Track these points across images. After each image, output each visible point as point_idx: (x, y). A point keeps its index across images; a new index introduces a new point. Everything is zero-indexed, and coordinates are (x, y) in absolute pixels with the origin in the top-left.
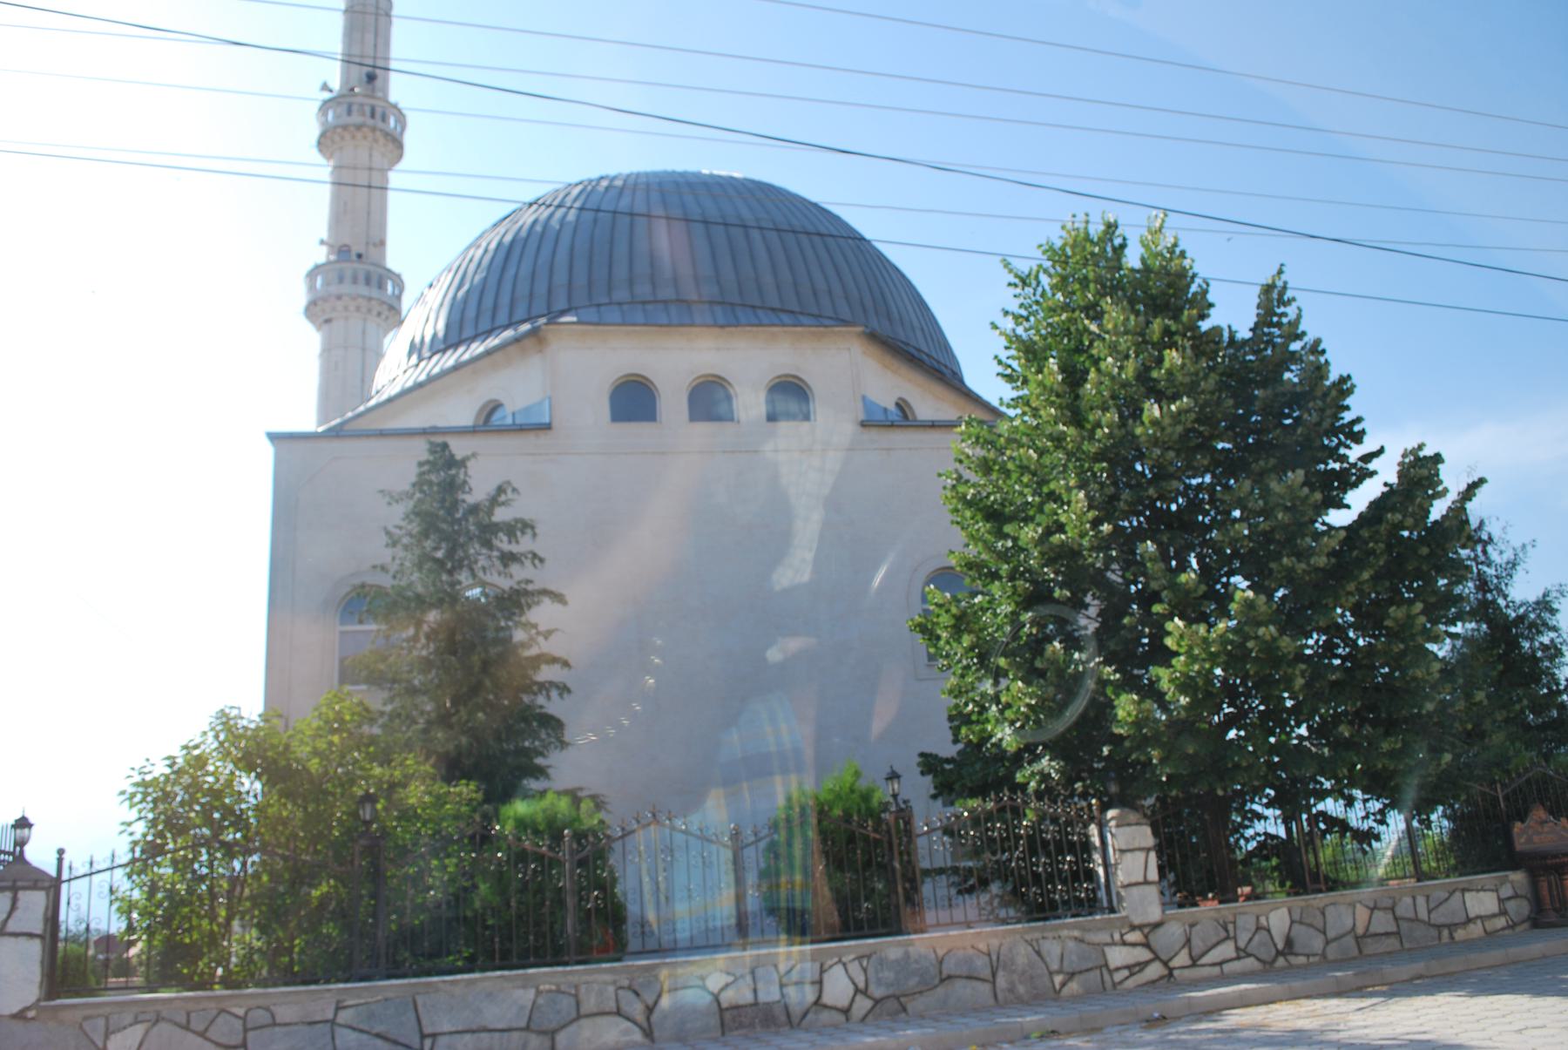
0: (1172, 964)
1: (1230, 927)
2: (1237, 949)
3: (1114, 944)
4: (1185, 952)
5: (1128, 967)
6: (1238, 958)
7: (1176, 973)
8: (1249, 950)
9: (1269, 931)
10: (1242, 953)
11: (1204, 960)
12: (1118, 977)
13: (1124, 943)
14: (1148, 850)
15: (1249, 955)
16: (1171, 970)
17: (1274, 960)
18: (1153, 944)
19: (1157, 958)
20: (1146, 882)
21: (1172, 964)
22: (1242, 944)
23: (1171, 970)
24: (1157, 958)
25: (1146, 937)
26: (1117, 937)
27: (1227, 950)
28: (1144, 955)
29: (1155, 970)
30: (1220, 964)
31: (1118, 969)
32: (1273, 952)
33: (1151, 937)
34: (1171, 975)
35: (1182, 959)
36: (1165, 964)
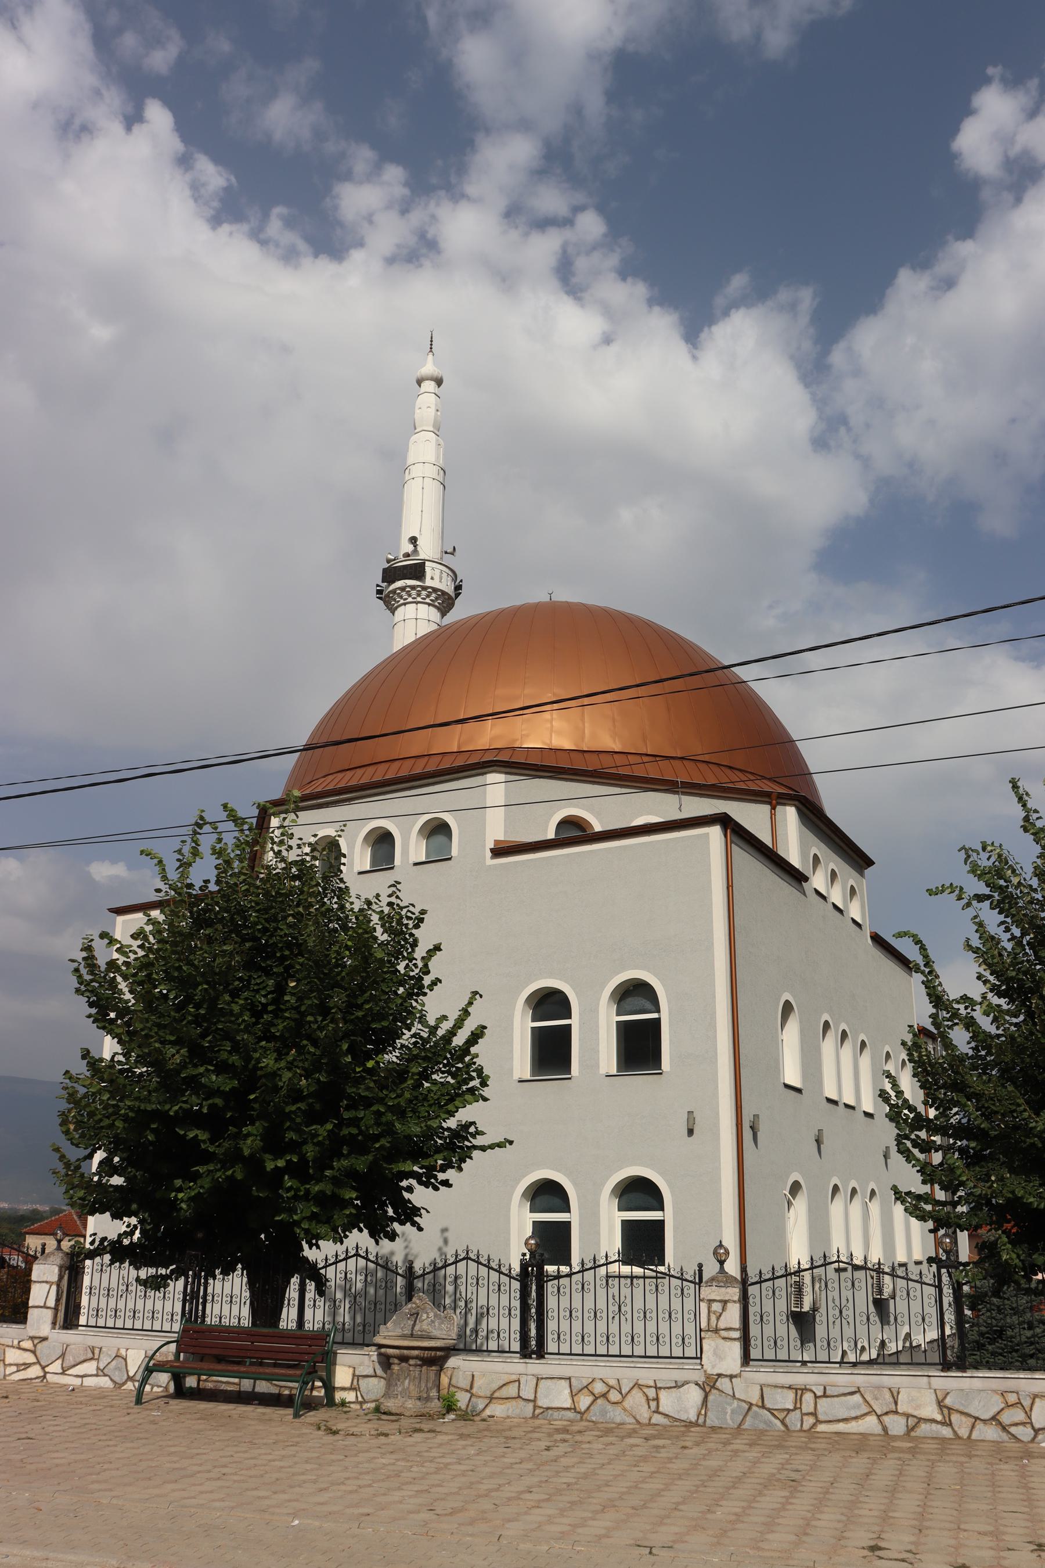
0: (47, 1369)
1: (97, 1351)
2: (98, 1368)
3: (13, 1347)
4: (59, 1362)
5: (17, 1365)
6: (97, 1375)
7: (48, 1376)
8: (106, 1371)
9: (125, 1360)
10: (101, 1372)
11: (69, 1372)
12: (9, 1370)
13: (19, 1348)
14: (51, 1284)
15: (105, 1375)
16: (46, 1373)
17: (124, 1384)
18: (38, 1353)
19: (38, 1362)
20: (45, 1307)
21: (47, 1369)
22: (102, 1367)
23: (46, 1373)
24: (38, 1362)
25: (35, 1346)
26: (16, 1342)
27: (90, 1367)
28: (30, 1358)
29: (35, 1371)
30: (82, 1377)
31: (10, 1365)
32: (125, 1377)
33: (39, 1346)
34: (44, 1377)
35: (56, 1367)
36: (43, 1368)
